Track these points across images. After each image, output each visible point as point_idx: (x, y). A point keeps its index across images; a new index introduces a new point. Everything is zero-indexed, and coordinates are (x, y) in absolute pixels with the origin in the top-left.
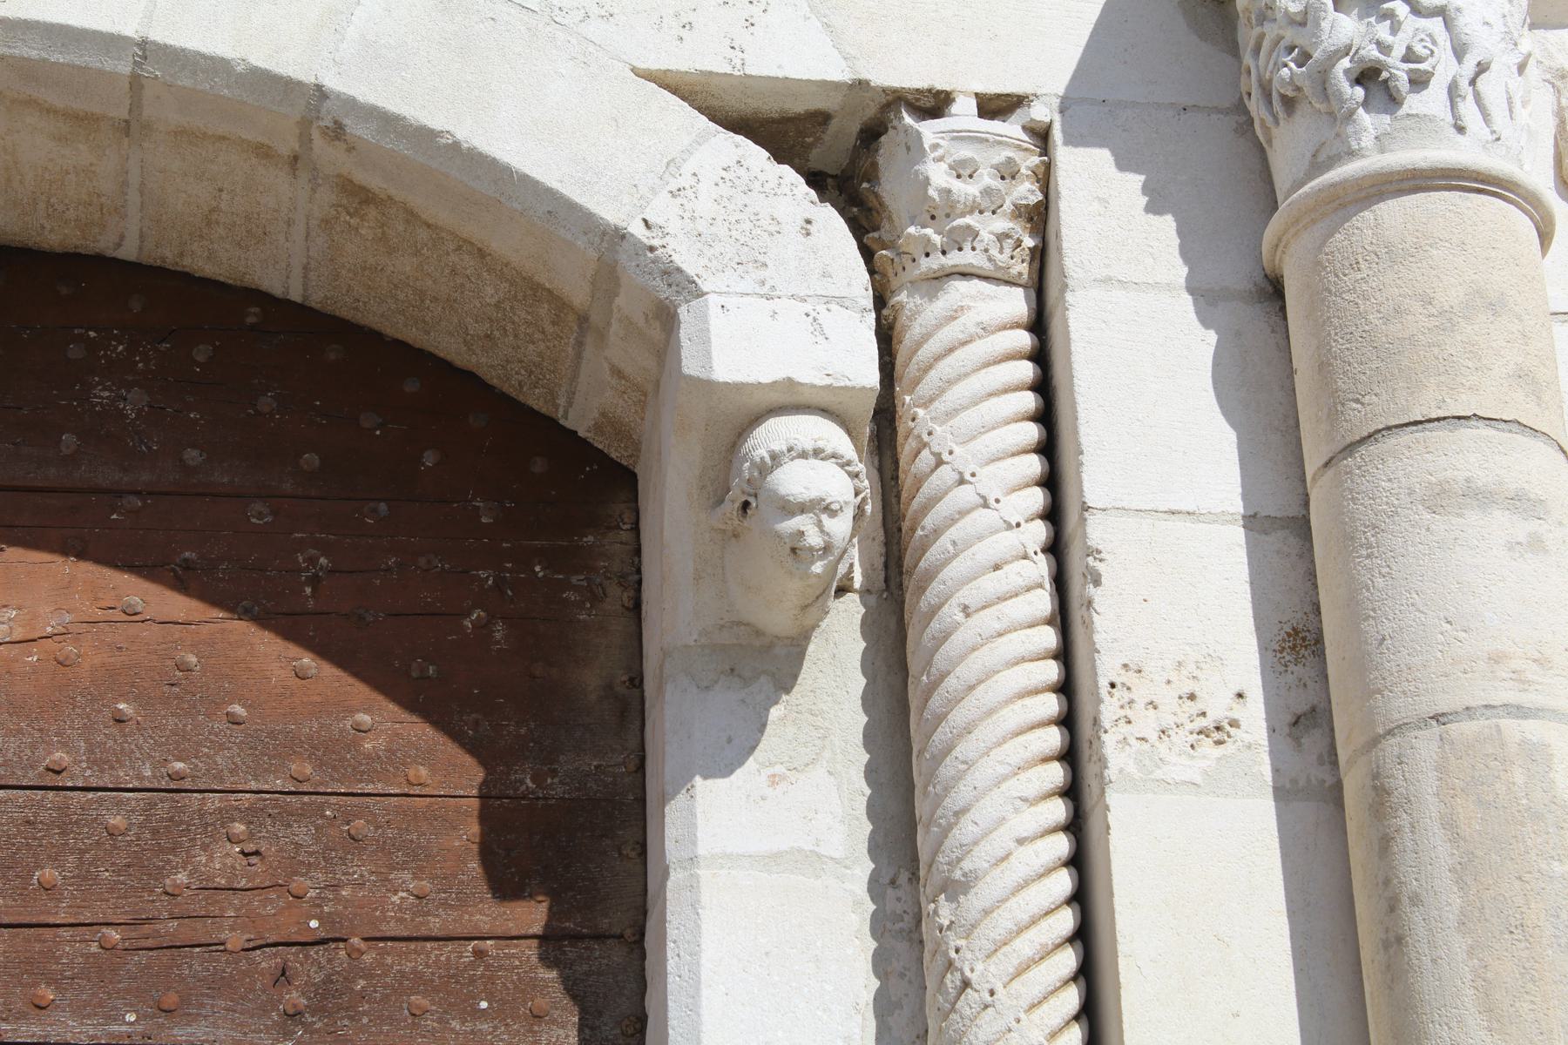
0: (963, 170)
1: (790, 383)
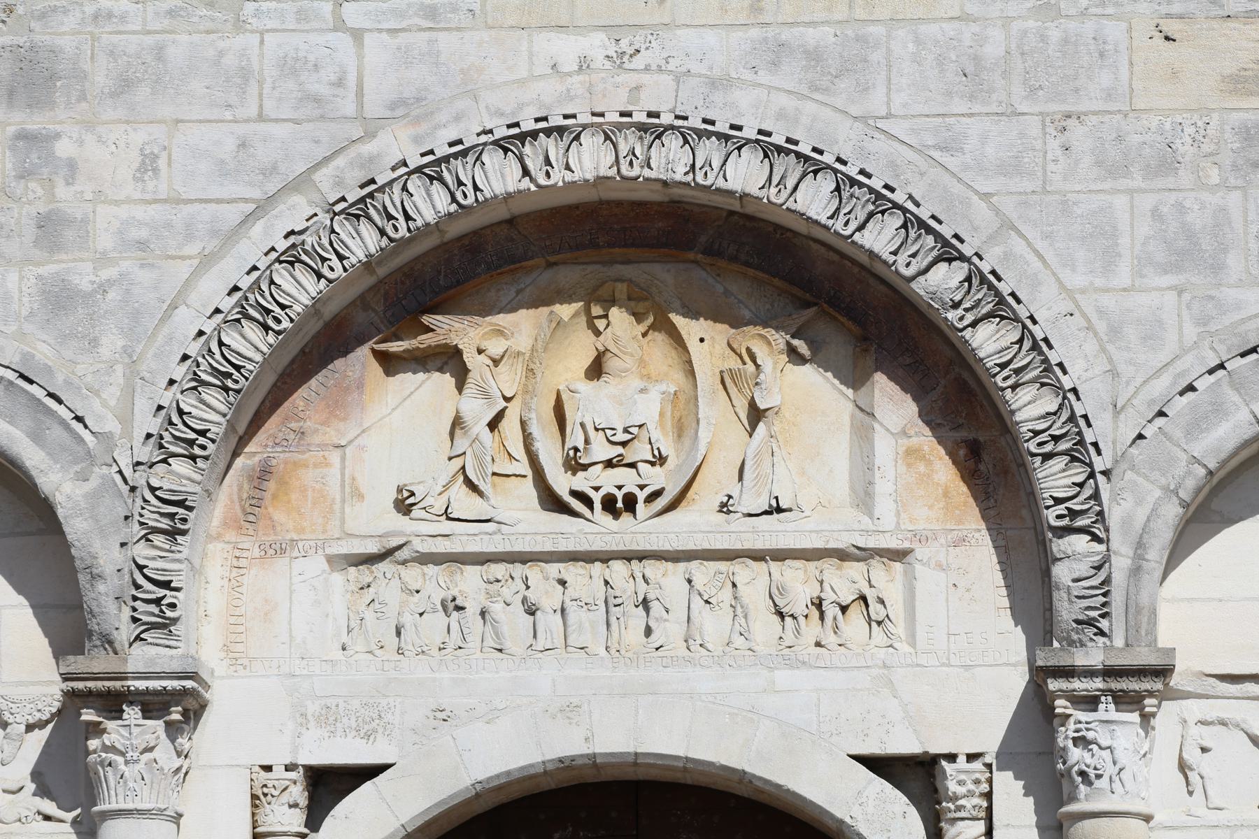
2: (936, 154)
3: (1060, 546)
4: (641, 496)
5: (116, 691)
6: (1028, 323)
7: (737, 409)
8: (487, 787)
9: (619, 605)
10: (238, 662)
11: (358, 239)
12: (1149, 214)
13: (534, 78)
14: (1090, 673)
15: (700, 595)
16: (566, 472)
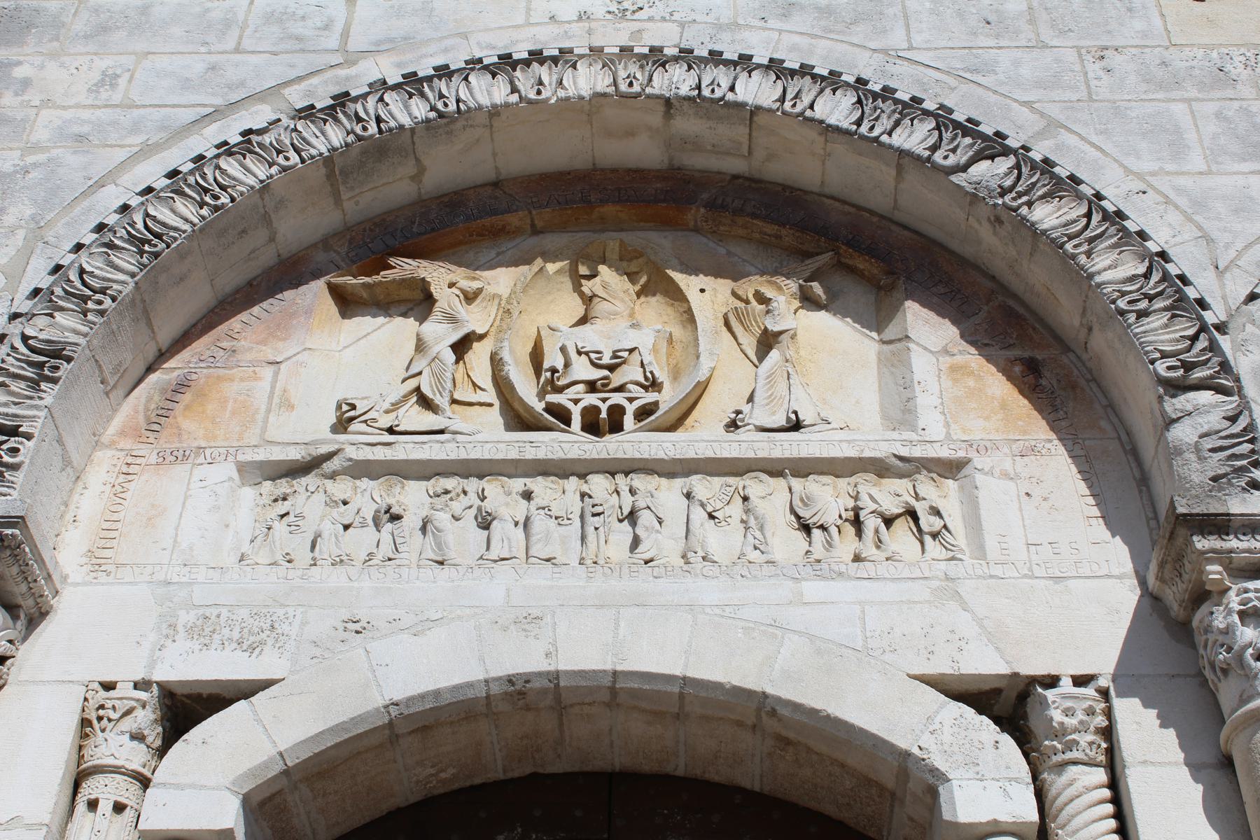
0: (1068, 712)
1: (995, 822)
7: (743, 347)
8: (406, 712)
9: (599, 514)
10: (102, 569)
11: (322, 138)
12: (1214, 116)
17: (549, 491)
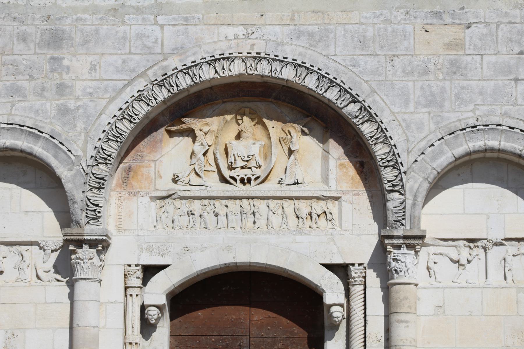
0: (356, 273)
1: (334, 303)
2: (351, 68)
3: (389, 196)
4: (253, 178)
5: (81, 239)
6: (380, 123)
7: (284, 150)
11: (161, 93)
12: (420, 88)
13: (219, 41)
14: (398, 238)
15: (272, 211)
16: (228, 170)
17: (232, 205)
